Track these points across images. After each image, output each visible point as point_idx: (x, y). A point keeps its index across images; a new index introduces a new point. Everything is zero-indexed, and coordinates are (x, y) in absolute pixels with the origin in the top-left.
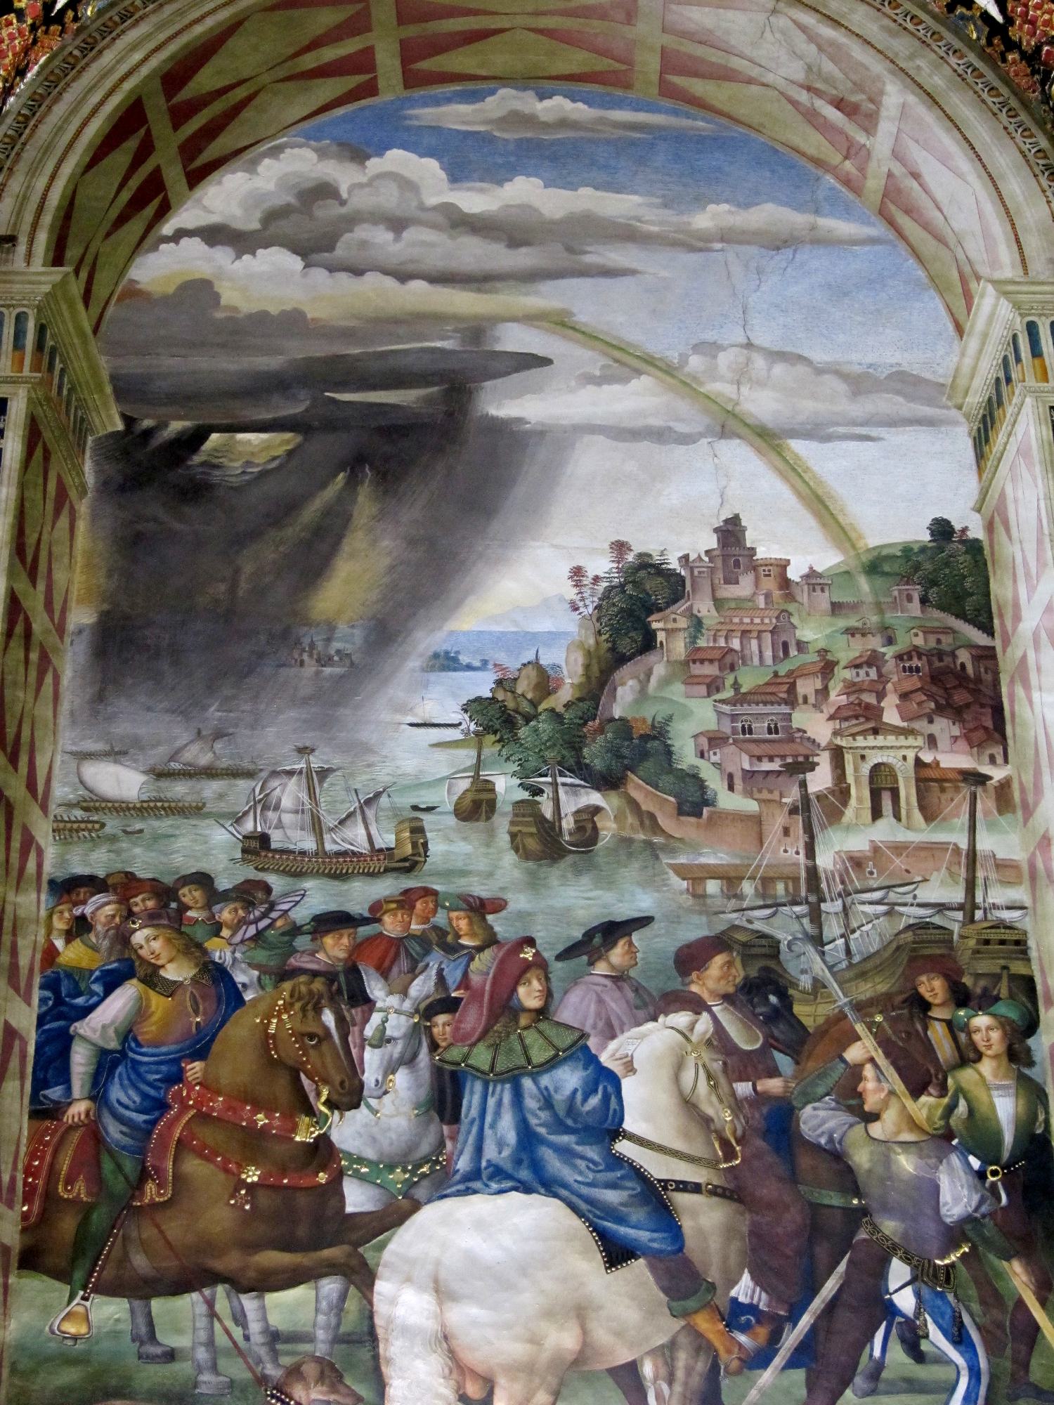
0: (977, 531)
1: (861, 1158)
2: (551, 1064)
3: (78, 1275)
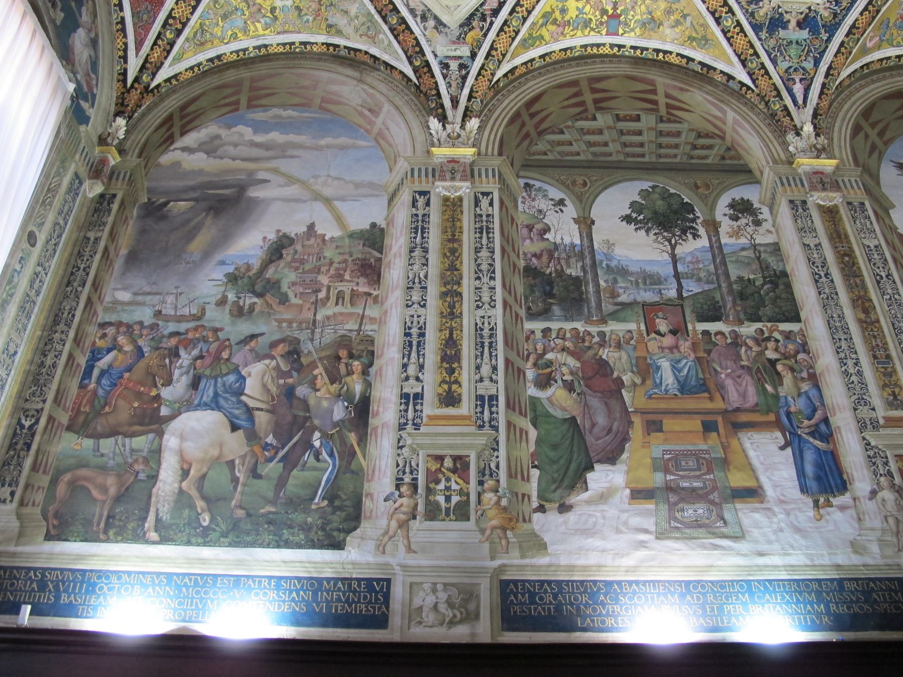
0: (384, 225)
1: (312, 402)
2: (227, 374)
3: (81, 432)
